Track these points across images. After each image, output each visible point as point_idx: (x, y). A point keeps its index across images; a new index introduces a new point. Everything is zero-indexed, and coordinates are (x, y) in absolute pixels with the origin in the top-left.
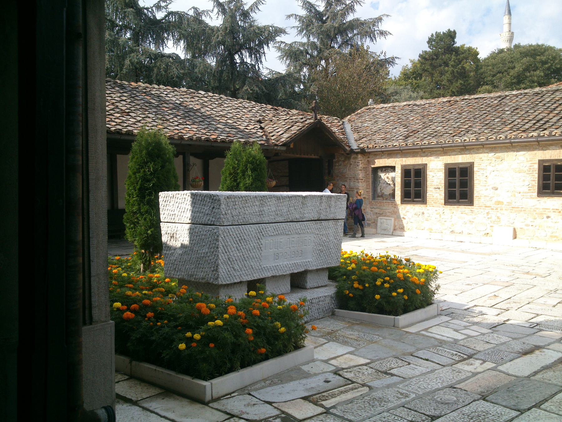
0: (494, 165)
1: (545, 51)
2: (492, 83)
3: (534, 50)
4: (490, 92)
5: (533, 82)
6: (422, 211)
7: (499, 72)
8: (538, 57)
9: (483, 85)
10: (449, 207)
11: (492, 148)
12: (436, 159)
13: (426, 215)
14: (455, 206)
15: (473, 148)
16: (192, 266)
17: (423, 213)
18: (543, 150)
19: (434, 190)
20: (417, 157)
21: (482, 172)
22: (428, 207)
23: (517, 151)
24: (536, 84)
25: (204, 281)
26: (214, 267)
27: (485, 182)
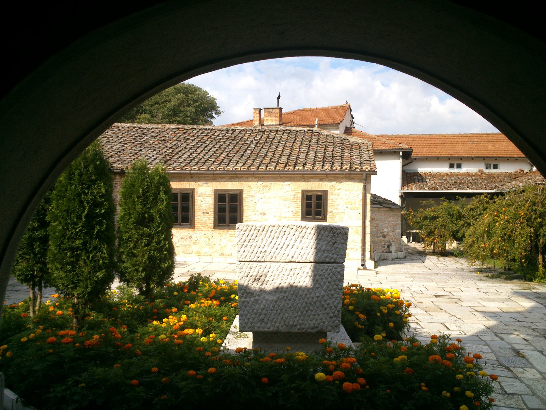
2: (151, 112)
3: (187, 88)
4: (149, 122)
5: (187, 116)
6: (189, 235)
7: (157, 103)
8: (190, 95)
9: (141, 113)
10: (218, 231)
12: (205, 185)
13: (194, 239)
15: (243, 177)
17: (191, 237)
18: (305, 181)
20: (184, 181)
21: (251, 198)
23: (283, 182)
24: (189, 118)
25: (314, 331)
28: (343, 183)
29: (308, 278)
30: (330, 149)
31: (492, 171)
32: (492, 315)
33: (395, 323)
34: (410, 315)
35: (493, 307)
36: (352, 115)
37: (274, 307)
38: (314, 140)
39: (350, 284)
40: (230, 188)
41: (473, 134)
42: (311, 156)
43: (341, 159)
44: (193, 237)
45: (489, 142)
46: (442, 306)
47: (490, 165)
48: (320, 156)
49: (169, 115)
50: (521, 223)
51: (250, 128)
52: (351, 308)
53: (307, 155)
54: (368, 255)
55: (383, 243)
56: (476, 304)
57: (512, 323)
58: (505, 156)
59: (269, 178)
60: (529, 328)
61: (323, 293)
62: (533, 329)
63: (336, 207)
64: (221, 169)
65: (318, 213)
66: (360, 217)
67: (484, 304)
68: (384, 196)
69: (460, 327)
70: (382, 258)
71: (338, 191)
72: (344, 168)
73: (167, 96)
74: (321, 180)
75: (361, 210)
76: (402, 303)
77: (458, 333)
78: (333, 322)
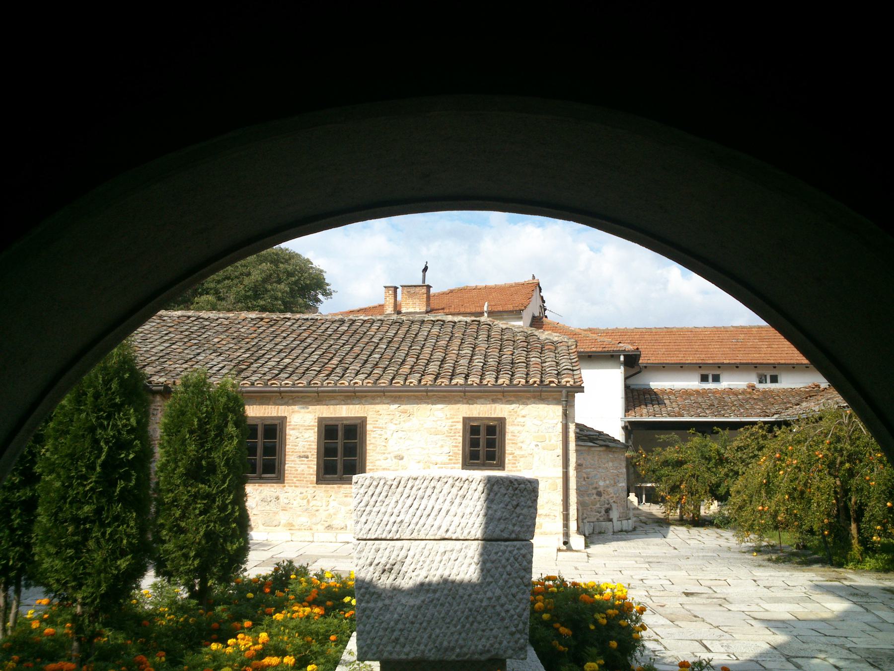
0: (397, 422)
1: (290, 259)
2: (217, 292)
4: (213, 308)
5: (276, 299)
6: (276, 495)
7: (228, 278)
8: (281, 265)
9: (201, 294)
11: (396, 397)
12: (303, 410)
13: (283, 500)
14: (335, 486)
15: (366, 396)
16: (453, 629)
17: (277, 498)
19: (297, 459)
21: (379, 431)
22: (287, 488)
25: (484, 658)
26: (516, 626)
27: (383, 448)
28: (529, 406)
29: (473, 566)
30: (507, 351)
31: (769, 386)
32: (780, 625)
33: (619, 642)
34: (643, 628)
35: (781, 611)
36: (542, 297)
37: (416, 617)
38: (483, 336)
39: (544, 576)
40: (344, 415)
41: (736, 327)
42: (478, 362)
43: (527, 367)
44: (281, 499)
45: (762, 339)
46: (697, 610)
47: (765, 376)
48: (492, 362)
49: (246, 297)
50: (820, 471)
51: (379, 317)
52: (546, 616)
53: (471, 360)
54: (573, 525)
55: (598, 506)
56: (754, 608)
57: (813, 638)
58: (789, 362)
59: (409, 397)
60: (842, 646)
61: (498, 592)
62: (849, 649)
63: (520, 445)
64: (330, 384)
65: (491, 456)
66: (560, 461)
67: (767, 606)
68: (598, 428)
69: (728, 647)
70: (597, 531)
71: (522, 420)
72: (531, 381)
73: (245, 266)
74: (494, 401)
75: (560, 451)
76: (631, 607)
77: (725, 657)
78: (516, 642)
